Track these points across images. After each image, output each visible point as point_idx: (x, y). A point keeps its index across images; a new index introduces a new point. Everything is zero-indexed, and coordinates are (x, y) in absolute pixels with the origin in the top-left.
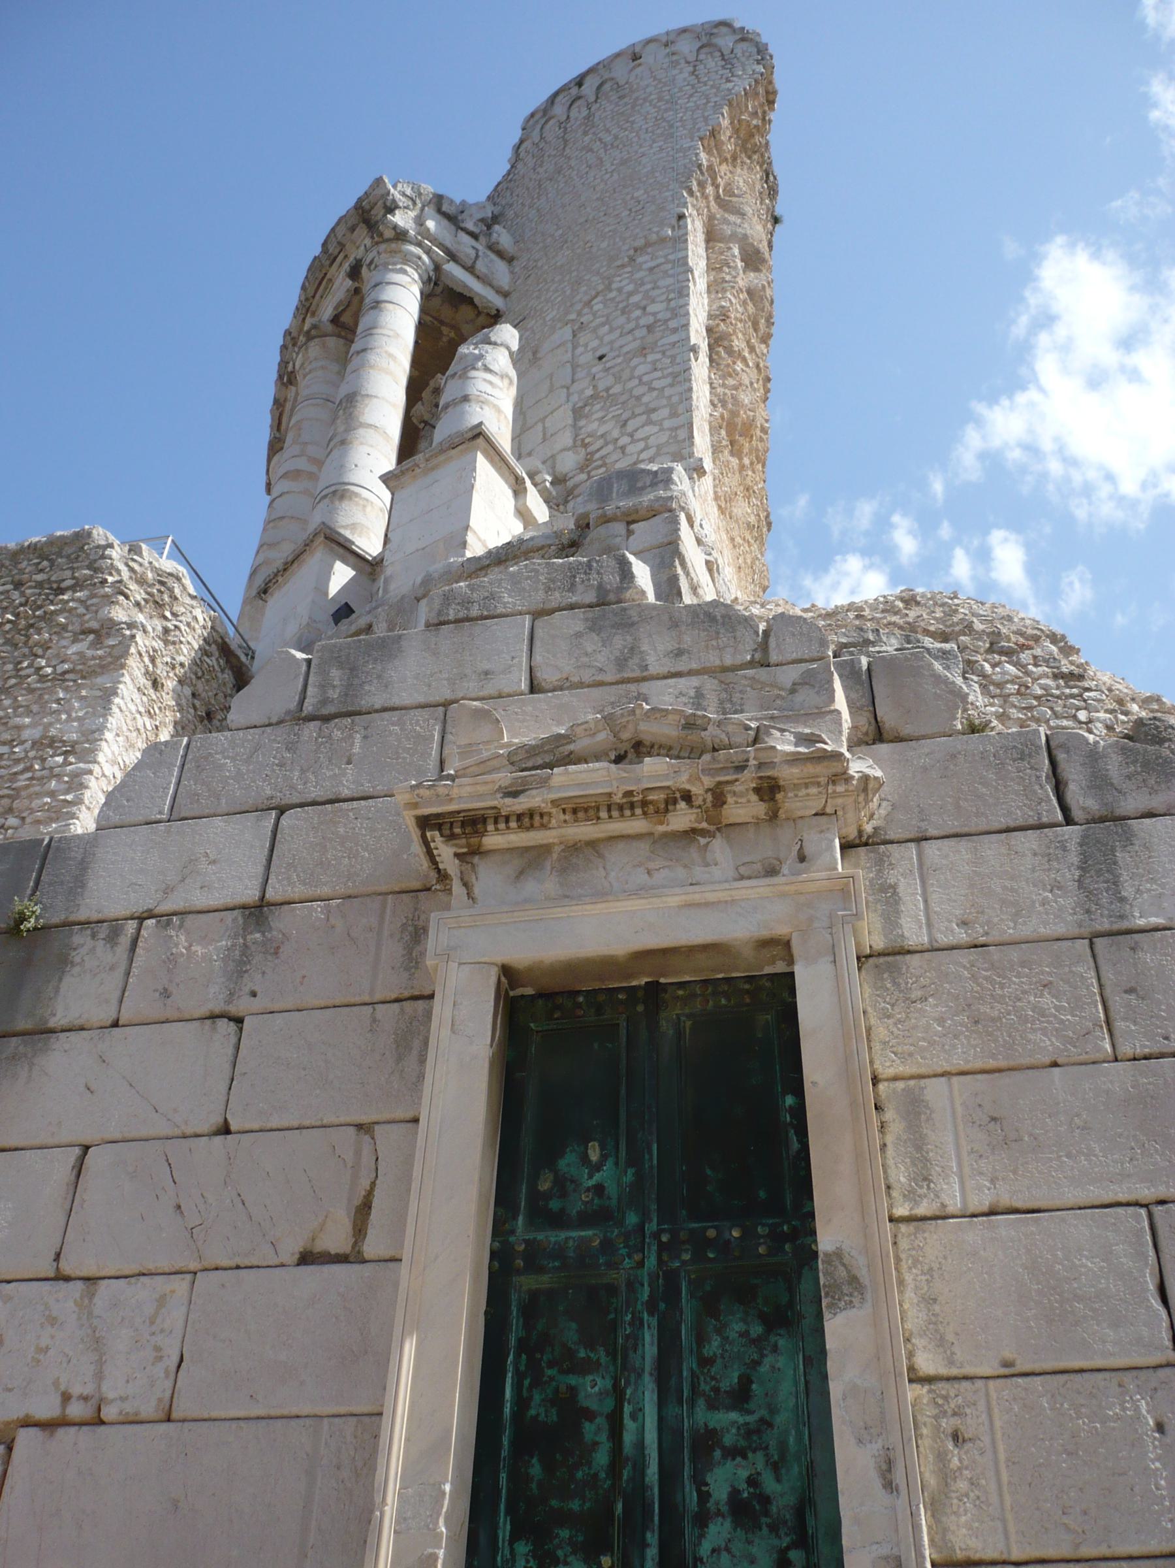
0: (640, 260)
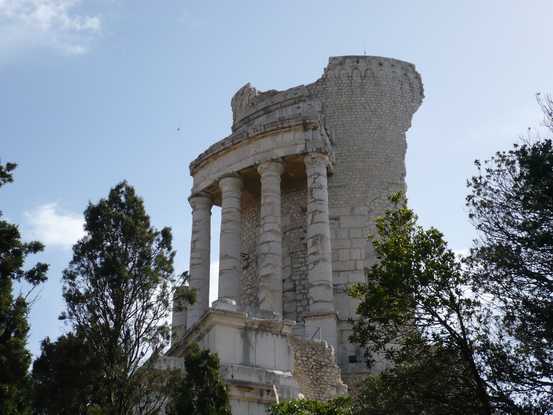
0: (390, 189)
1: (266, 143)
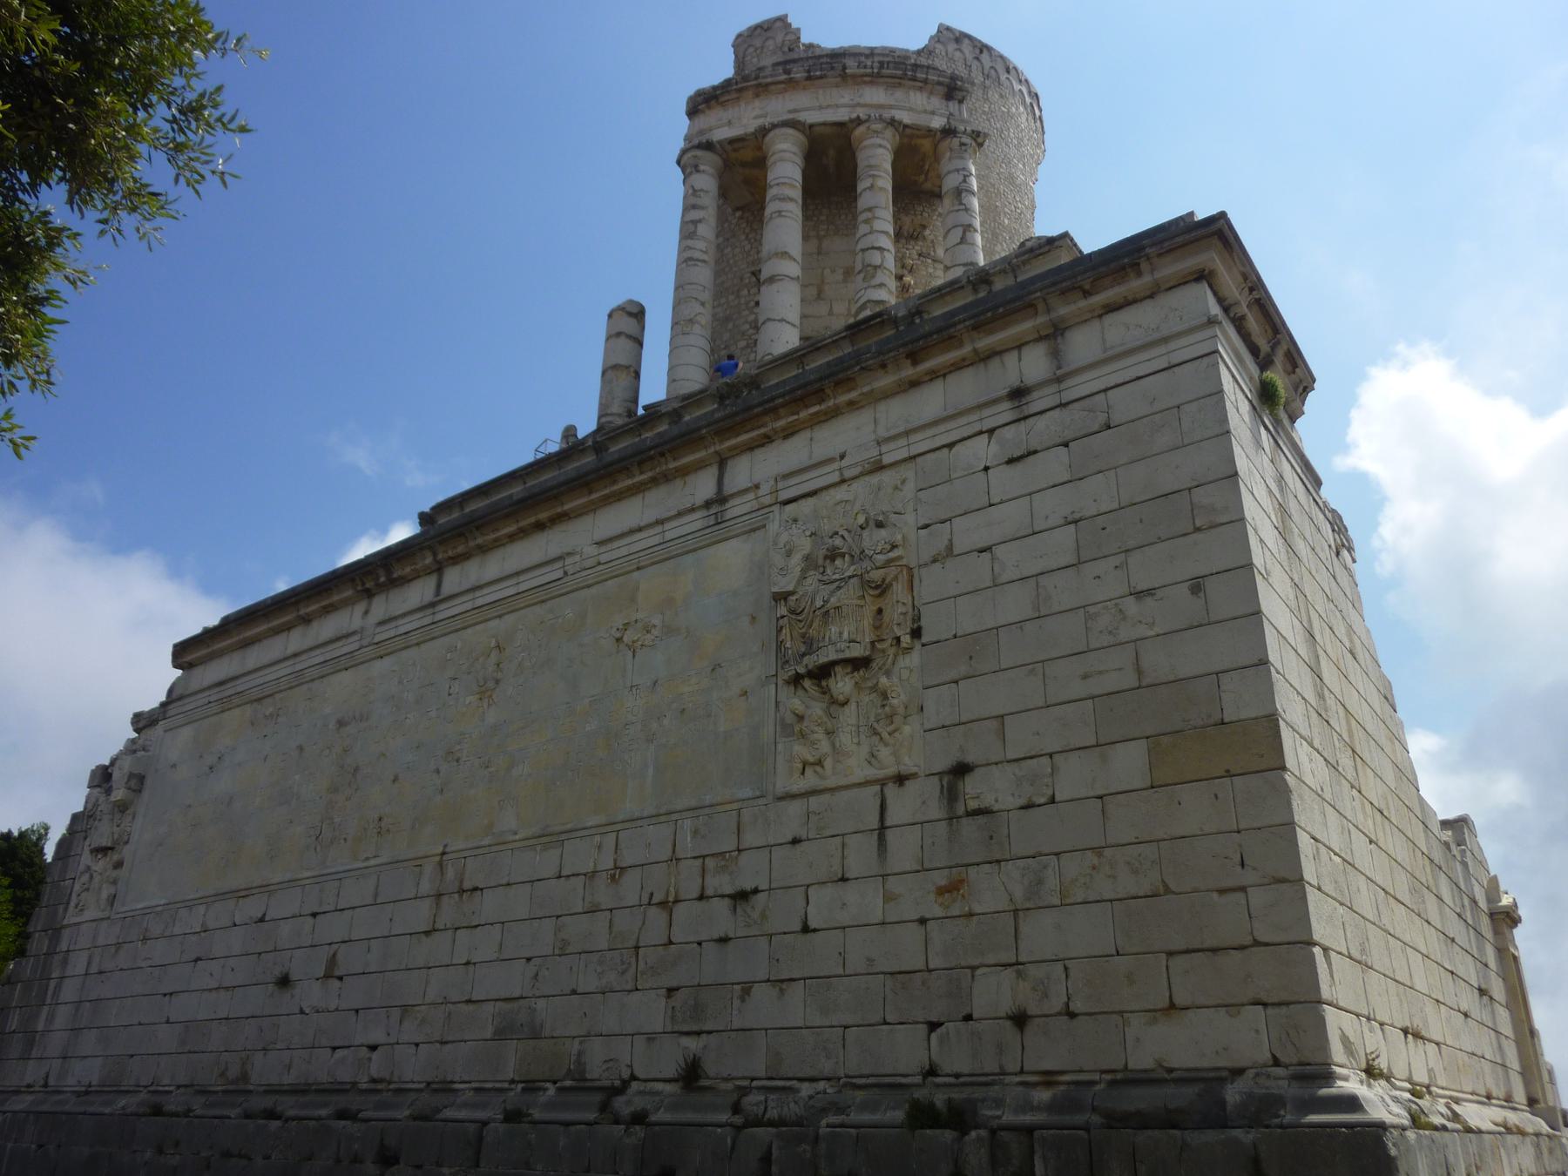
1: (875, 95)
